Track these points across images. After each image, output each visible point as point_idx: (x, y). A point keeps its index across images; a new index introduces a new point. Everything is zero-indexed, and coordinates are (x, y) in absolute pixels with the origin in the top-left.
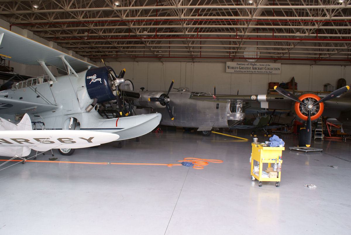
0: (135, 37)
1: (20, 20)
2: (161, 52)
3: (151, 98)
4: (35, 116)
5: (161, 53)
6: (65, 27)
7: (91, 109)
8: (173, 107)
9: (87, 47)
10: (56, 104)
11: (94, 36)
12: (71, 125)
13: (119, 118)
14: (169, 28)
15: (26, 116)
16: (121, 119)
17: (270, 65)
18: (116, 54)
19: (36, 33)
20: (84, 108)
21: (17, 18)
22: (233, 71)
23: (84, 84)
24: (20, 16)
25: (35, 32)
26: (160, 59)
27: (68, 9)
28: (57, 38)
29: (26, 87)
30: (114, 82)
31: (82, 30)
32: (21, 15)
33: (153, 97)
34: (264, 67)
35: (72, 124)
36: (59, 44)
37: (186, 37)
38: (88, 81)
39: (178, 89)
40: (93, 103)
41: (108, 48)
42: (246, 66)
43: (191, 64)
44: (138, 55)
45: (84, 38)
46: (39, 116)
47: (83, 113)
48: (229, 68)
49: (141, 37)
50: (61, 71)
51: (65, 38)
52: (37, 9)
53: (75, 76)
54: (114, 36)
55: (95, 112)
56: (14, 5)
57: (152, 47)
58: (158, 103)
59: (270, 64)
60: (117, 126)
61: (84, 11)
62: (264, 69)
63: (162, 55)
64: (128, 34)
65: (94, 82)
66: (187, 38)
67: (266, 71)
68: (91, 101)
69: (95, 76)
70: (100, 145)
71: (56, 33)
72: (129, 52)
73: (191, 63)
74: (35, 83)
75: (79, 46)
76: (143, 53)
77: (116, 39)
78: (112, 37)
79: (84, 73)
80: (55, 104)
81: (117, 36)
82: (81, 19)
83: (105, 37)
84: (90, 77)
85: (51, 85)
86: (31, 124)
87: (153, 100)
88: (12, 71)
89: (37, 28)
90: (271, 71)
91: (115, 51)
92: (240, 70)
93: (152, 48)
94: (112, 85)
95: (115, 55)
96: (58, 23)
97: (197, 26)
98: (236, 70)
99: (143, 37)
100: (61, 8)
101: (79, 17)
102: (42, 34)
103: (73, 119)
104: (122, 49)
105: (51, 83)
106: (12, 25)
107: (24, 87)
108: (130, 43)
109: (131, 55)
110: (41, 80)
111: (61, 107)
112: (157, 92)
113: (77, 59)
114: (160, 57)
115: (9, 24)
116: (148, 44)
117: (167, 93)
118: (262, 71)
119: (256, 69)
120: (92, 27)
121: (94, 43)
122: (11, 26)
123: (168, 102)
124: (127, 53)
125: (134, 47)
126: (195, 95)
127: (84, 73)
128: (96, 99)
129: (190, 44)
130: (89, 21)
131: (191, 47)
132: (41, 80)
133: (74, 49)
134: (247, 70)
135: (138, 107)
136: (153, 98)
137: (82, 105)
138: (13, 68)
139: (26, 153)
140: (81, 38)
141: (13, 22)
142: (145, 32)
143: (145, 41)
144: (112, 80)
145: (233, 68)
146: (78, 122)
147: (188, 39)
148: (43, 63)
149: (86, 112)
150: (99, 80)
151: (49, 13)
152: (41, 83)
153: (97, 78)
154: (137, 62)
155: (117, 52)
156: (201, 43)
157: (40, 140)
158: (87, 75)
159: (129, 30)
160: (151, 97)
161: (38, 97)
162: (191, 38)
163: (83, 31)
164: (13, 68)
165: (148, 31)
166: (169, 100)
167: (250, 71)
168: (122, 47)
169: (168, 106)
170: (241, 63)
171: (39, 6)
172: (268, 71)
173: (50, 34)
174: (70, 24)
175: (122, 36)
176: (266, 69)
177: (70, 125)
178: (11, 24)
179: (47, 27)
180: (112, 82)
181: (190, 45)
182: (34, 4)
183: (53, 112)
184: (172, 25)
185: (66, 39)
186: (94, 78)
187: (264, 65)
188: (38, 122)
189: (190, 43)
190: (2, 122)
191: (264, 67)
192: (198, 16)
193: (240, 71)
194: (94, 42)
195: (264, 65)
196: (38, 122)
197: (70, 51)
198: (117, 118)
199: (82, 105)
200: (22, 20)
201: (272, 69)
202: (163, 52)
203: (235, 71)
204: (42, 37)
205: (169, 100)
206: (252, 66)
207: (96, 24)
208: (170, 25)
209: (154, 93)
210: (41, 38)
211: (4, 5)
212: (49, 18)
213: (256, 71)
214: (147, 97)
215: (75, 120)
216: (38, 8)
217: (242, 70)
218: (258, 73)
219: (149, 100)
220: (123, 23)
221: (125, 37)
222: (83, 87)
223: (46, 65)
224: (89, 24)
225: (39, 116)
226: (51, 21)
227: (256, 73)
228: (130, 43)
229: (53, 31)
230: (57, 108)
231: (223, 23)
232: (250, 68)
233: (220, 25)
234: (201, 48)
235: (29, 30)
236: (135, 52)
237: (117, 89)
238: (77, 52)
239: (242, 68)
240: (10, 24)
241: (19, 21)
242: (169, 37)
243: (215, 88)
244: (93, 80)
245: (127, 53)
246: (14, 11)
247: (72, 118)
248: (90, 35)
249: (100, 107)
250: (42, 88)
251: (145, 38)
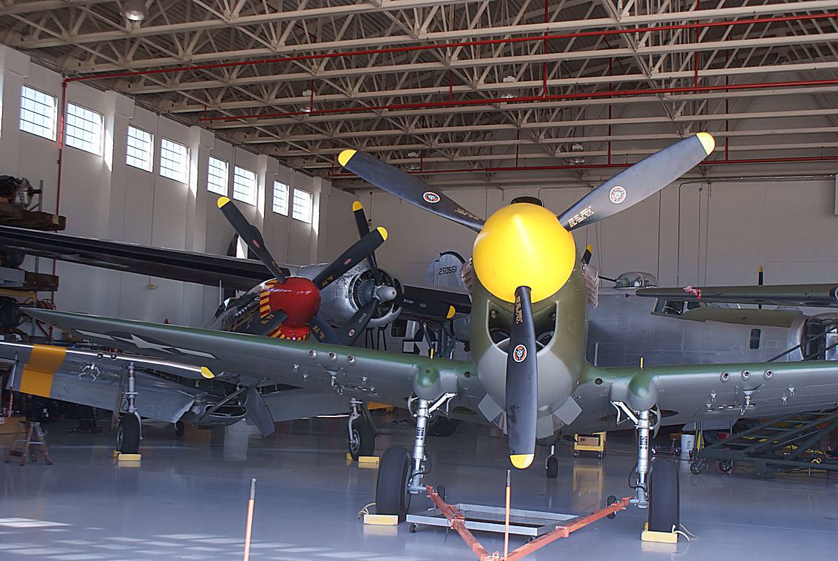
0: (473, 98)
1: (92, 61)
2: (581, 147)
5: (580, 150)
6: (234, 75)
8: (597, 345)
9: (317, 141)
11: (339, 103)
14: (609, 60)
18: (419, 160)
19: (146, 102)
21: (84, 57)
24: (91, 51)
25: (140, 99)
26: (581, 174)
27: (233, 17)
28: (215, 115)
31: (293, 82)
32: (93, 46)
36: (224, 136)
37: (662, 87)
39: (615, 281)
41: (391, 140)
43: (701, 189)
44: (502, 160)
45: (302, 110)
49: (494, 97)
51: (239, 114)
52: (138, 25)
54: (406, 97)
56: (73, 16)
57: (541, 130)
61: (289, 20)
63: (582, 158)
64: (446, 89)
66: (661, 92)
71: (209, 97)
72: (464, 152)
73: (699, 185)
75: (290, 139)
76: (514, 156)
77: (414, 108)
78: (397, 103)
81: (417, 98)
82: (279, 46)
83: (371, 105)
88: (62, 226)
89: (147, 83)
91: (416, 151)
93: (542, 136)
95: (417, 164)
96: (211, 65)
97: (723, 44)
99: (503, 97)
100: (214, 17)
101: (275, 41)
102: (166, 104)
104: (435, 144)
106: (68, 80)
108: (469, 118)
109: (474, 162)
114: (582, 166)
115: (59, 78)
116: (525, 120)
120: (319, 71)
121: (339, 127)
122: (64, 85)
124: (457, 157)
125: (486, 132)
126: (673, 303)
129: (679, 113)
130: (310, 53)
131: (687, 123)
133: (273, 151)
138: (62, 219)
140: (292, 110)
141: (72, 69)
142: (510, 78)
143: (516, 112)
147: (668, 97)
151: (181, 36)
154: (499, 186)
155: (424, 153)
156: (610, 111)
159: (451, 77)
162: (678, 92)
163: (298, 87)
164: (62, 219)
165: (518, 78)
168: (435, 135)
171: (145, 15)
173: (190, 102)
174: (249, 66)
175: (435, 95)
178: (67, 77)
179: (177, 80)
181: (678, 118)
182: (130, 9)
184: (617, 47)
185: (244, 118)
189: (677, 109)
192: (697, 9)
194: (337, 122)
197: (260, 156)
200: (99, 61)
202: (587, 146)
204: (162, 115)
207: (335, 59)
208: (610, 48)
210: (161, 116)
211: (43, 22)
212: (181, 51)
216: (143, 22)
220: (428, 51)
221: (438, 101)
224: (313, 64)
226: (185, 59)
228: (469, 118)
229: (196, 92)
231: (824, 24)
233: (801, 33)
234: (610, 129)
235: (121, 92)
236: (491, 150)
238: (284, 160)
240: (64, 76)
241: (91, 67)
242: (609, 90)
243: (761, 274)
245: (457, 157)
246: (73, 35)
248: (317, 98)
251: (509, 101)
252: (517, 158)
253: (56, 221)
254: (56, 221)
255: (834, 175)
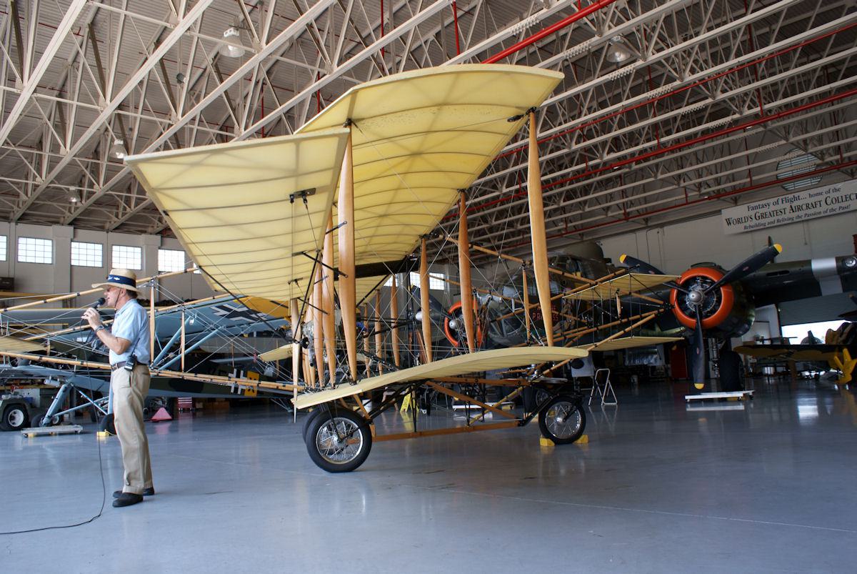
17: (838, 190)
22: (740, 228)
34: (822, 198)
42: (772, 208)
43: (658, 232)
48: (729, 223)
59: (839, 186)
62: (823, 203)
67: (830, 207)
73: (656, 230)
90: (843, 205)
92: (757, 222)
98: (747, 224)
118: (818, 209)
119: (799, 208)
134: (776, 218)
145: (739, 221)
167: (783, 220)
170: (757, 204)
172: (836, 206)
176: (829, 202)
187: (821, 194)
191: (822, 198)
193: (759, 225)
195: (821, 194)
201: (848, 198)
203: (745, 228)
206: (787, 206)
213: (801, 213)
217: (762, 221)
218: (841, 211)
227: (838, 211)
232: (782, 211)
239: (763, 216)
255: (720, 211)
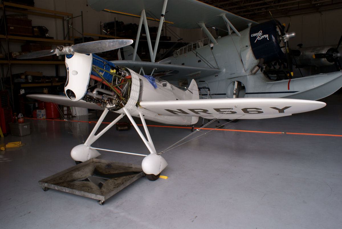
3: (315, 55)
4: (199, 81)
7: (257, 71)
10: (218, 67)
12: (236, 89)
13: (291, 80)
15: (193, 83)
16: (294, 80)
18: (266, 10)
20: (249, 71)
23: (248, 43)
29: (187, 52)
30: (283, 38)
33: (317, 53)
35: (236, 88)
38: (252, 39)
40: (259, 63)
41: (257, 5)
46: (204, 81)
47: (248, 76)
50: (221, 32)
53: (237, 35)
55: (260, 74)
58: (324, 60)
60: (289, 89)
63: (320, 3)
65: (260, 39)
68: (256, 62)
69: (261, 32)
70: (291, 115)
74: (195, 47)
76: (298, 5)
79: (248, 31)
80: (217, 67)
84: (254, 35)
85: (212, 48)
86: (198, 89)
87: (319, 56)
88: (170, 40)
94: (280, 41)
95: (265, 12)
103: (237, 82)
105: (212, 45)
107: (185, 52)
109: (283, 9)
110: (201, 44)
111: (224, 70)
112: (323, 47)
113: (238, 16)
117: (337, 47)
123: (338, 57)
124: (278, 8)
127: (248, 31)
128: (262, 59)
132: (201, 44)
135: (298, 66)
136: (318, 54)
137: (246, 67)
139: (194, 120)
144: (280, 36)
146: (242, 85)
148: (204, 25)
149: (251, 74)
150: (266, 37)
152: (201, 47)
153: (263, 35)
157: (221, 110)
158: (252, 32)
160: (315, 53)
161: (199, 61)
164: (170, 38)
166: (339, 55)
169: (337, 63)
177: (235, 89)
180: (280, 38)
183: (215, 76)
186: (259, 35)
188: (204, 88)
190: (173, 90)
196: (204, 88)
198: (289, 80)
199: (246, 67)
205: (339, 55)
209: (319, 49)
214: (311, 54)
215: (239, 83)
219: (314, 57)
222: (247, 46)
223: (206, 26)
225: (204, 81)
230: (220, 72)
237: (286, 45)
244: (258, 38)
245: (278, 8)
247: (236, 82)
249: (266, 68)
250: (203, 51)
252: (299, 6)
253: (168, 38)
254: (168, 38)
